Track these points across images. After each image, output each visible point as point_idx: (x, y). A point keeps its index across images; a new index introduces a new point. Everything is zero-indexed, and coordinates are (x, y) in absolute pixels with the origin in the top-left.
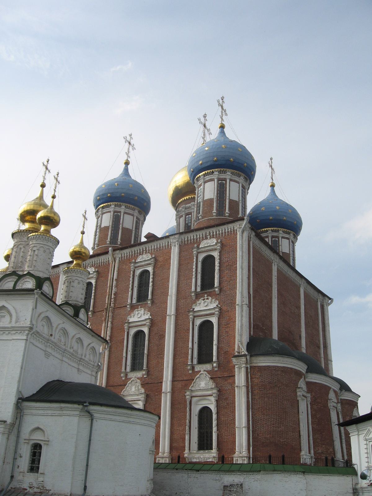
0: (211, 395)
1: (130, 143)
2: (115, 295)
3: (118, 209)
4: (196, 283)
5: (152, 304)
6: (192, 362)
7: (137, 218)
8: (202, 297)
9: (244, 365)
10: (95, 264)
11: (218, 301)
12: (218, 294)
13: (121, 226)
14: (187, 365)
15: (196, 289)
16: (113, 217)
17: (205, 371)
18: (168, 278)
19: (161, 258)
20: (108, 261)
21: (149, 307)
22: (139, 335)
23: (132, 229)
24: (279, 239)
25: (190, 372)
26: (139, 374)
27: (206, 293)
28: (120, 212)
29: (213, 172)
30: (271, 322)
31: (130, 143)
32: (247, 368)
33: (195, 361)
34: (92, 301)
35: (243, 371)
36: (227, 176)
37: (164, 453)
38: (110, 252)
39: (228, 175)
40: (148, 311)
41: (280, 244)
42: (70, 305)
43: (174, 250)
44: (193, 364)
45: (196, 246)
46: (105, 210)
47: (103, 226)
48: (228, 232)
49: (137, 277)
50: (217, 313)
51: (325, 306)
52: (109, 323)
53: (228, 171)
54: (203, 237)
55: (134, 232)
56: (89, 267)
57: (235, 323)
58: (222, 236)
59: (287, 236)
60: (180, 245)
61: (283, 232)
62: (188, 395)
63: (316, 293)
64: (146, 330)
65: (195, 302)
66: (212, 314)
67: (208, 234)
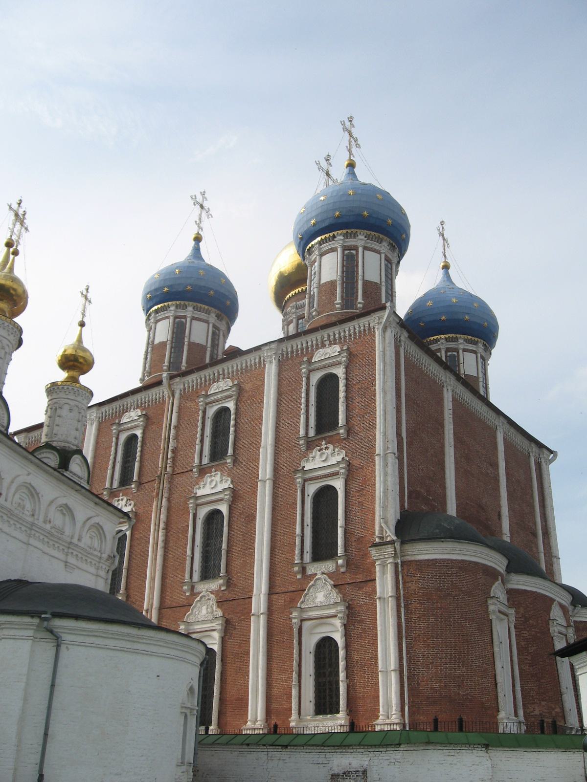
0: (336, 616)
1: (202, 207)
2: (173, 452)
3: (181, 312)
5: (234, 463)
6: (302, 559)
7: (214, 326)
8: (317, 446)
9: (391, 560)
10: (142, 404)
11: (344, 452)
12: (344, 439)
13: (186, 339)
14: (294, 565)
16: (174, 325)
17: (323, 573)
18: (261, 417)
19: (249, 385)
20: (163, 396)
21: (229, 470)
22: (214, 517)
23: (205, 344)
24: (458, 353)
25: (299, 576)
26: (215, 585)
27: (324, 438)
28: (185, 317)
29: (334, 237)
30: (443, 487)
31: (202, 207)
32: (396, 565)
33: (307, 557)
34: (137, 465)
35: (390, 569)
36: (359, 241)
37: (256, 721)
39: (360, 240)
40: (228, 476)
41: (461, 361)
42: (54, 448)
43: (269, 369)
44: (304, 562)
45: (305, 359)
46: (160, 316)
47: (157, 342)
48: (360, 332)
49: (209, 419)
50: (342, 471)
51: (544, 464)
52: (164, 500)
53: (360, 233)
54: (317, 345)
55: (209, 349)
56: (132, 410)
57: (375, 487)
58: (350, 339)
60: (279, 360)
61: (467, 341)
62: (295, 618)
63: (526, 443)
64: (224, 508)
65: (305, 456)
66: (335, 474)
67: (326, 339)
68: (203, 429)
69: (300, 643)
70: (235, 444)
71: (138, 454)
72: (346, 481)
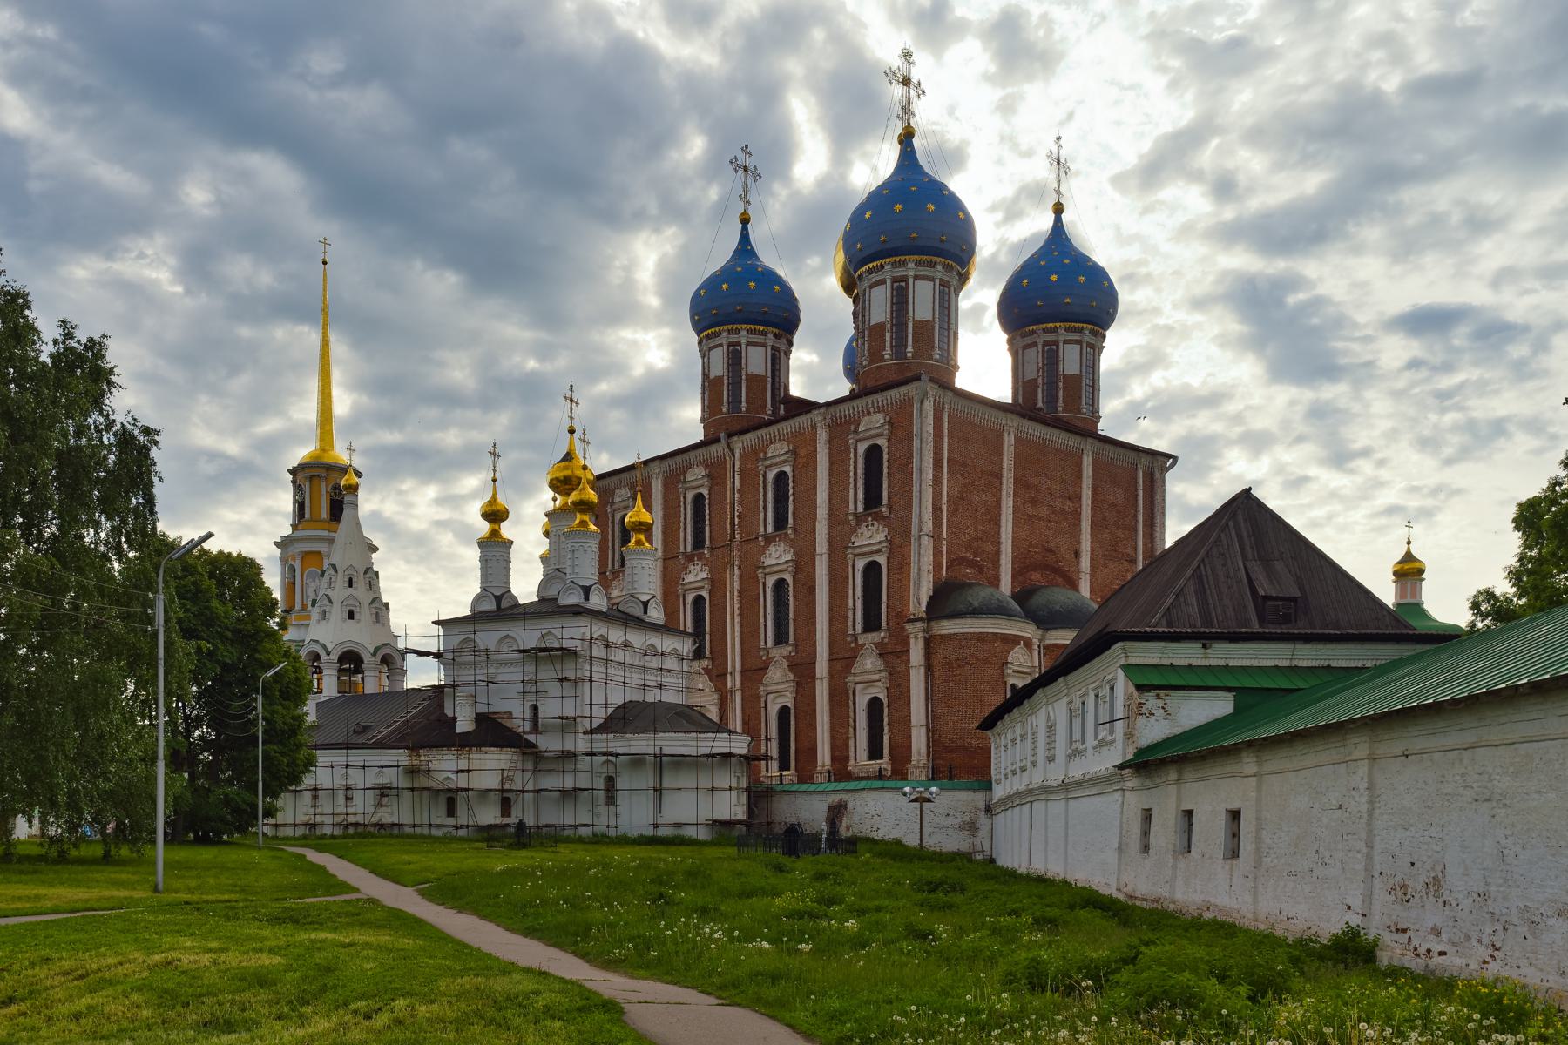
3: (734, 338)
4: (856, 499)
7: (773, 348)
13: (744, 373)
14: (848, 636)
15: (856, 508)
24: (1058, 346)
25: (853, 645)
26: (786, 650)
27: (870, 515)
28: (739, 344)
30: (997, 543)
34: (707, 529)
38: (723, 441)
45: (852, 428)
47: (712, 376)
55: (769, 379)
59: (1076, 336)
64: (788, 577)
65: (854, 531)
68: (765, 495)
69: (854, 703)
70: (794, 513)
71: (707, 518)
72: (888, 558)
